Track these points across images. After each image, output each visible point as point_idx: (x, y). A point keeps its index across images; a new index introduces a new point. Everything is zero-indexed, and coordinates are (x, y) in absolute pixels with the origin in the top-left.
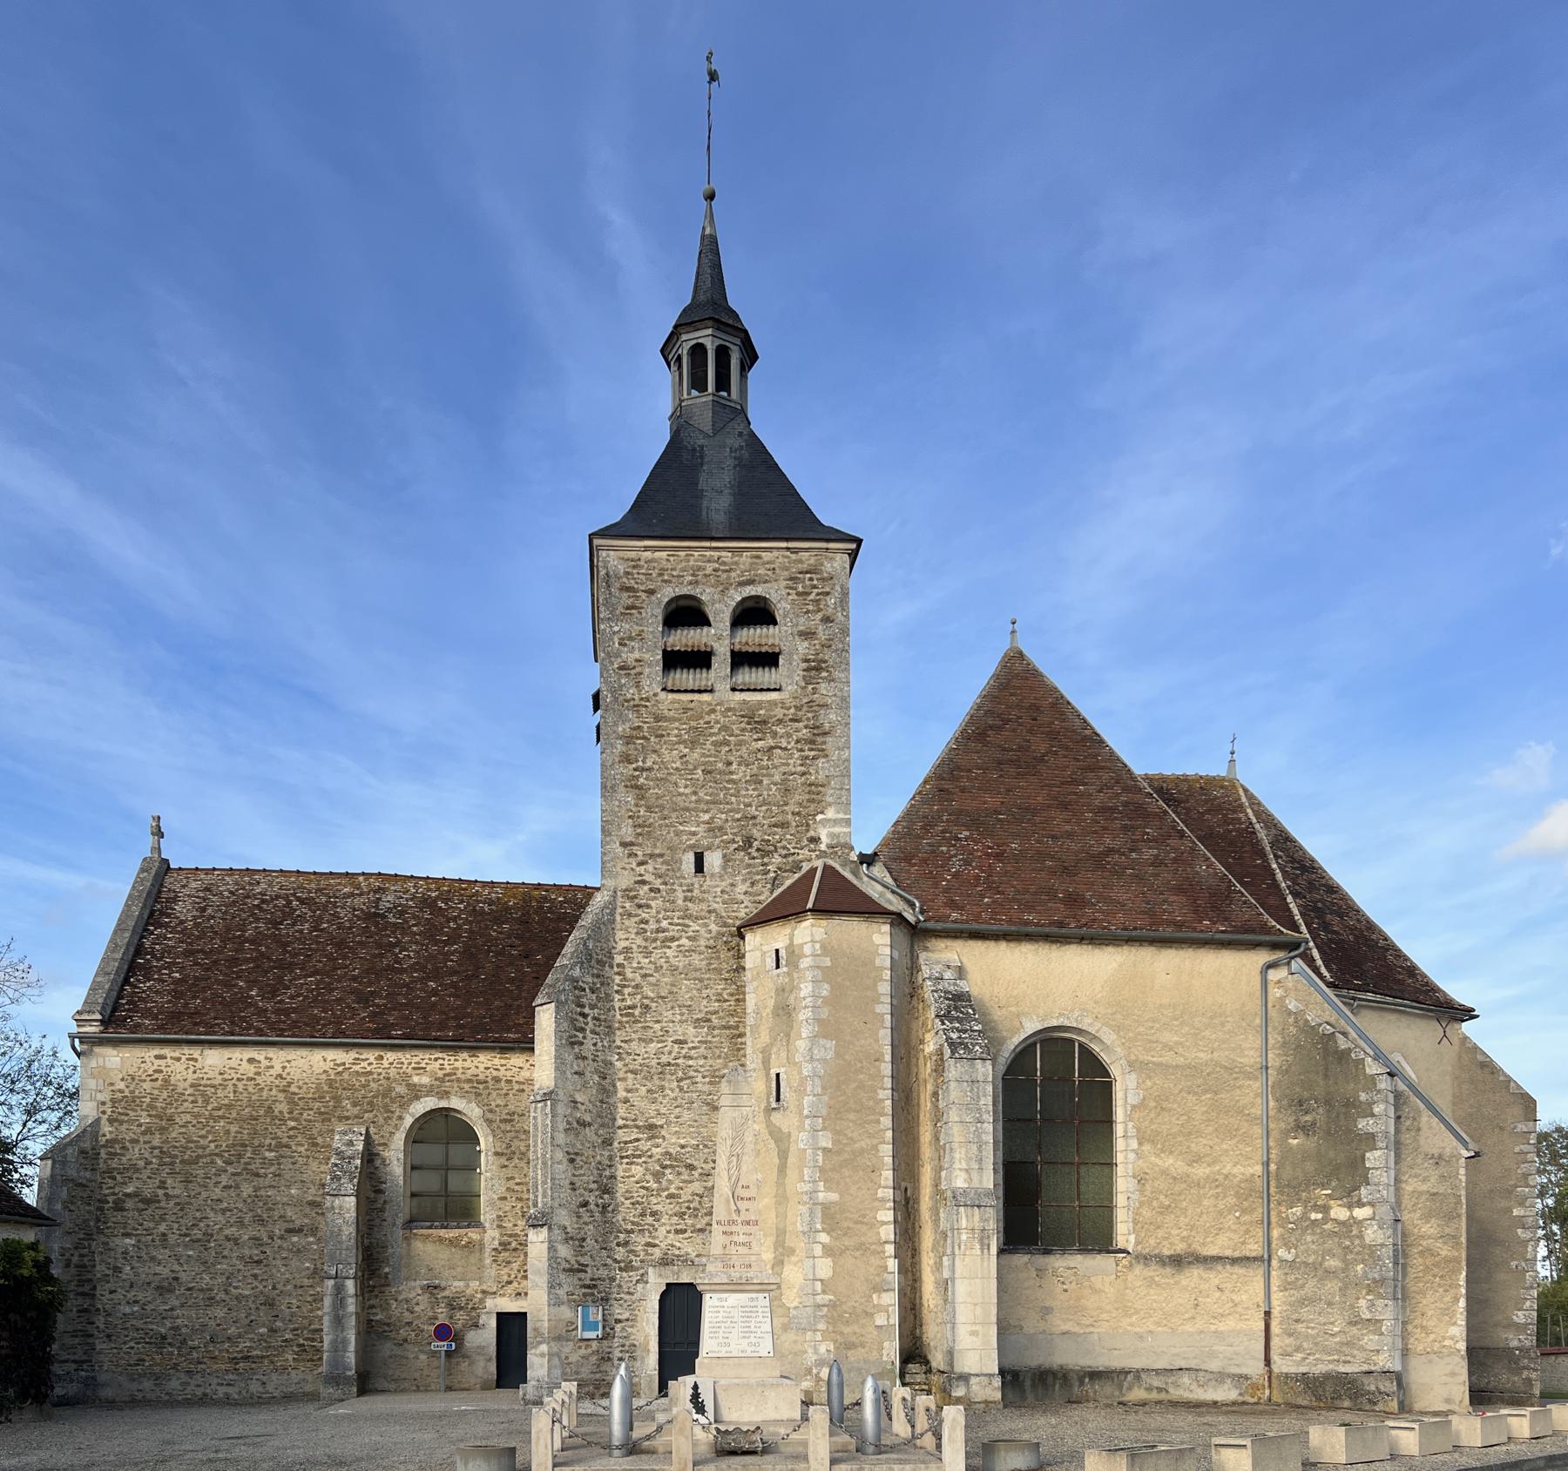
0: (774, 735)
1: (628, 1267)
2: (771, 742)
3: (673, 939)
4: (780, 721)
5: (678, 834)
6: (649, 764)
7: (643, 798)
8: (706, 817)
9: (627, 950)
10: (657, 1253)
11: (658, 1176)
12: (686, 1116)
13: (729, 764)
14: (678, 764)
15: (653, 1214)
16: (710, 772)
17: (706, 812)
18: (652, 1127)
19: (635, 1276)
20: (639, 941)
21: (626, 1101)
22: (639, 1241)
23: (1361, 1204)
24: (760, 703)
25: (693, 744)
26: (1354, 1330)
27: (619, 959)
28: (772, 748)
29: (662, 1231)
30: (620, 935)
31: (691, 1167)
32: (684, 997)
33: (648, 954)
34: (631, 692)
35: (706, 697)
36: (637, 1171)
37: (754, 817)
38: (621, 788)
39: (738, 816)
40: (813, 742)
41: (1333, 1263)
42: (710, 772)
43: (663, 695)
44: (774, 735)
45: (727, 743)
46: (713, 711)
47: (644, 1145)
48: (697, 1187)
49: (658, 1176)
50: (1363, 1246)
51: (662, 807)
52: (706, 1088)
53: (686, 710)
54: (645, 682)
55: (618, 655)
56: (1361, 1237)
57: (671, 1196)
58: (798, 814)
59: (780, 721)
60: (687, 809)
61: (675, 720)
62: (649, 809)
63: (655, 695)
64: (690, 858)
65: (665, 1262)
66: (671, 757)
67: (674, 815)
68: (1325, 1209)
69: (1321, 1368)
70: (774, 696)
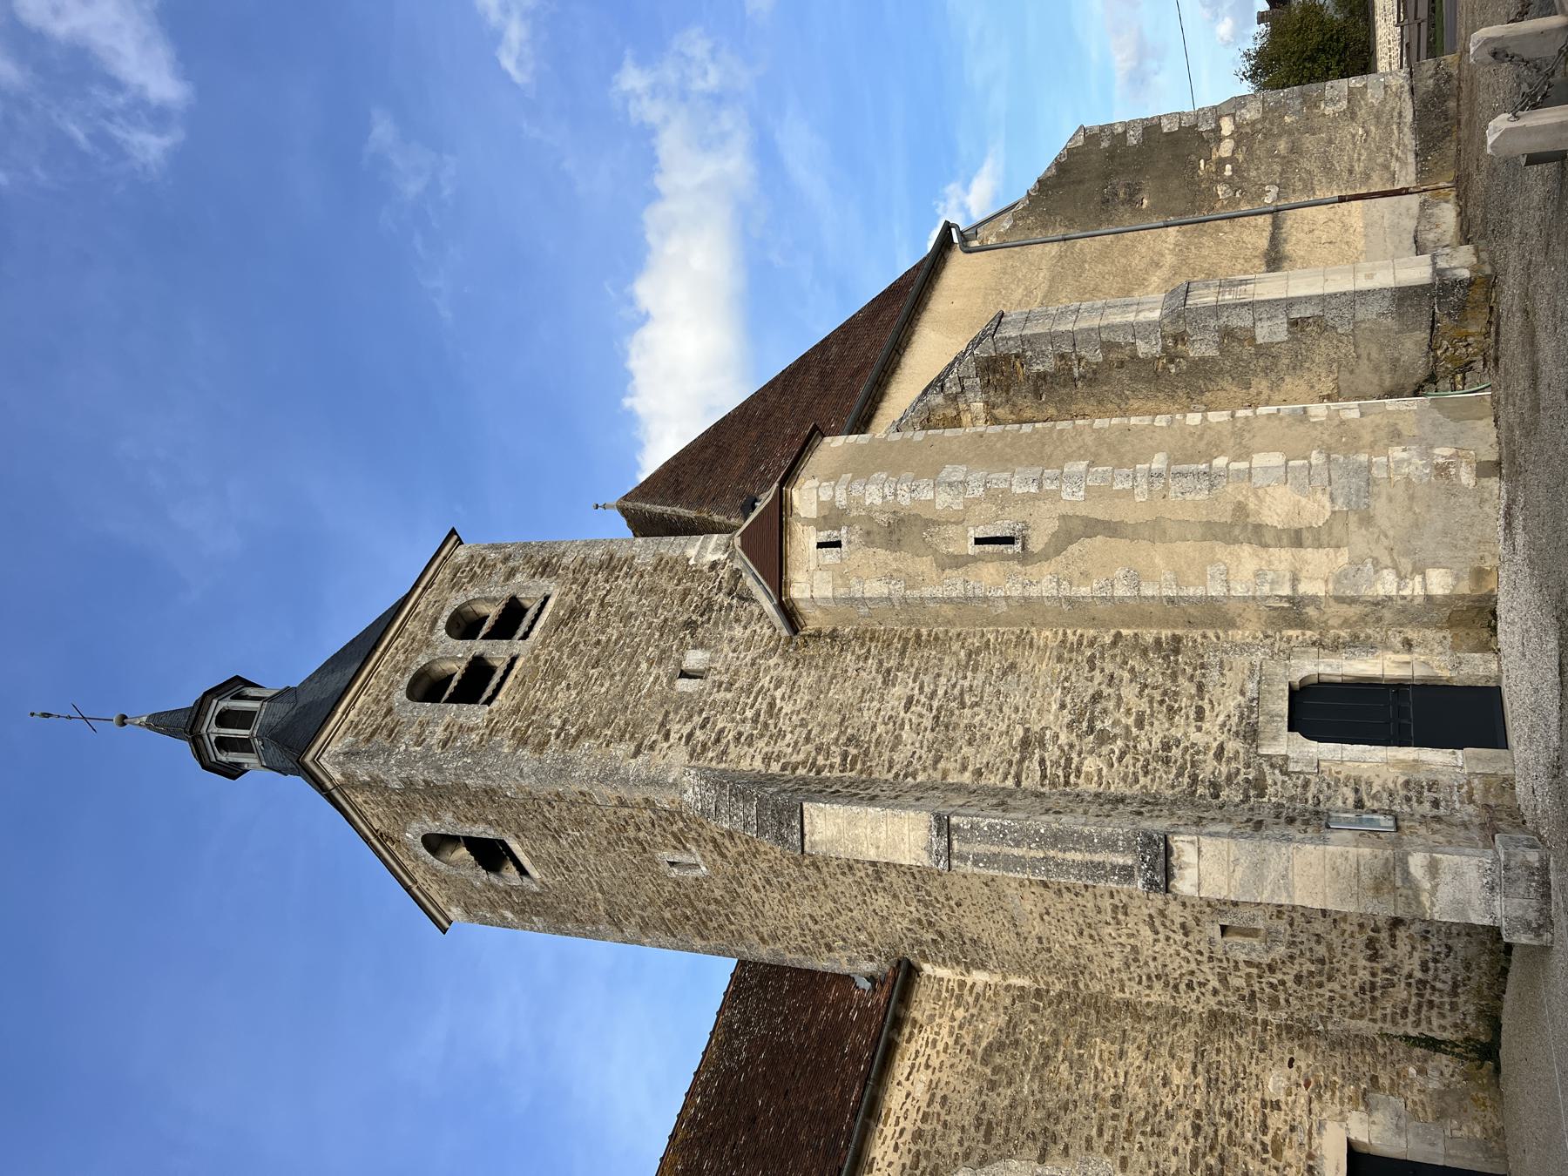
0: (590, 601)
1: (1259, 786)
2: (596, 605)
3: (772, 705)
4: (579, 597)
5: (650, 695)
6: (558, 723)
7: (593, 731)
8: (644, 666)
9: (767, 759)
10: (1233, 746)
11: (1104, 738)
12: (1017, 699)
13: (599, 642)
14: (574, 693)
15: (1166, 747)
16: (597, 662)
17: (638, 665)
18: (1025, 743)
19: (1272, 776)
20: (761, 744)
21: (978, 773)
22: (1209, 767)
23: (1219, 128)
24: (552, 614)
25: (561, 676)
26: (1362, 113)
27: (775, 768)
28: (602, 605)
29: (1195, 736)
30: (745, 765)
31: (1097, 697)
32: (850, 695)
33: (781, 734)
34: (475, 737)
35: (519, 664)
36: (1091, 764)
37: (666, 620)
38: (570, 753)
39: (657, 635)
40: (614, 568)
41: (1282, 146)
42: (597, 662)
43: (495, 705)
44: (590, 601)
45: (577, 644)
46: (537, 658)
47: (1052, 753)
48: (1129, 692)
49: (1104, 738)
50: (1264, 119)
51: (613, 710)
52: (981, 676)
53: (523, 683)
54: (474, 721)
55: (430, 748)
56: (1254, 123)
57: (1140, 723)
58: (679, 581)
59: (579, 597)
60: (626, 685)
61: (527, 693)
62: (607, 725)
63: (490, 712)
64: (683, 685)
65: (1251, 734)
66: (563, 697)
67: (627, 698)
68: (1222, 162)
69: (1409, 140)
70: (551, 602)
